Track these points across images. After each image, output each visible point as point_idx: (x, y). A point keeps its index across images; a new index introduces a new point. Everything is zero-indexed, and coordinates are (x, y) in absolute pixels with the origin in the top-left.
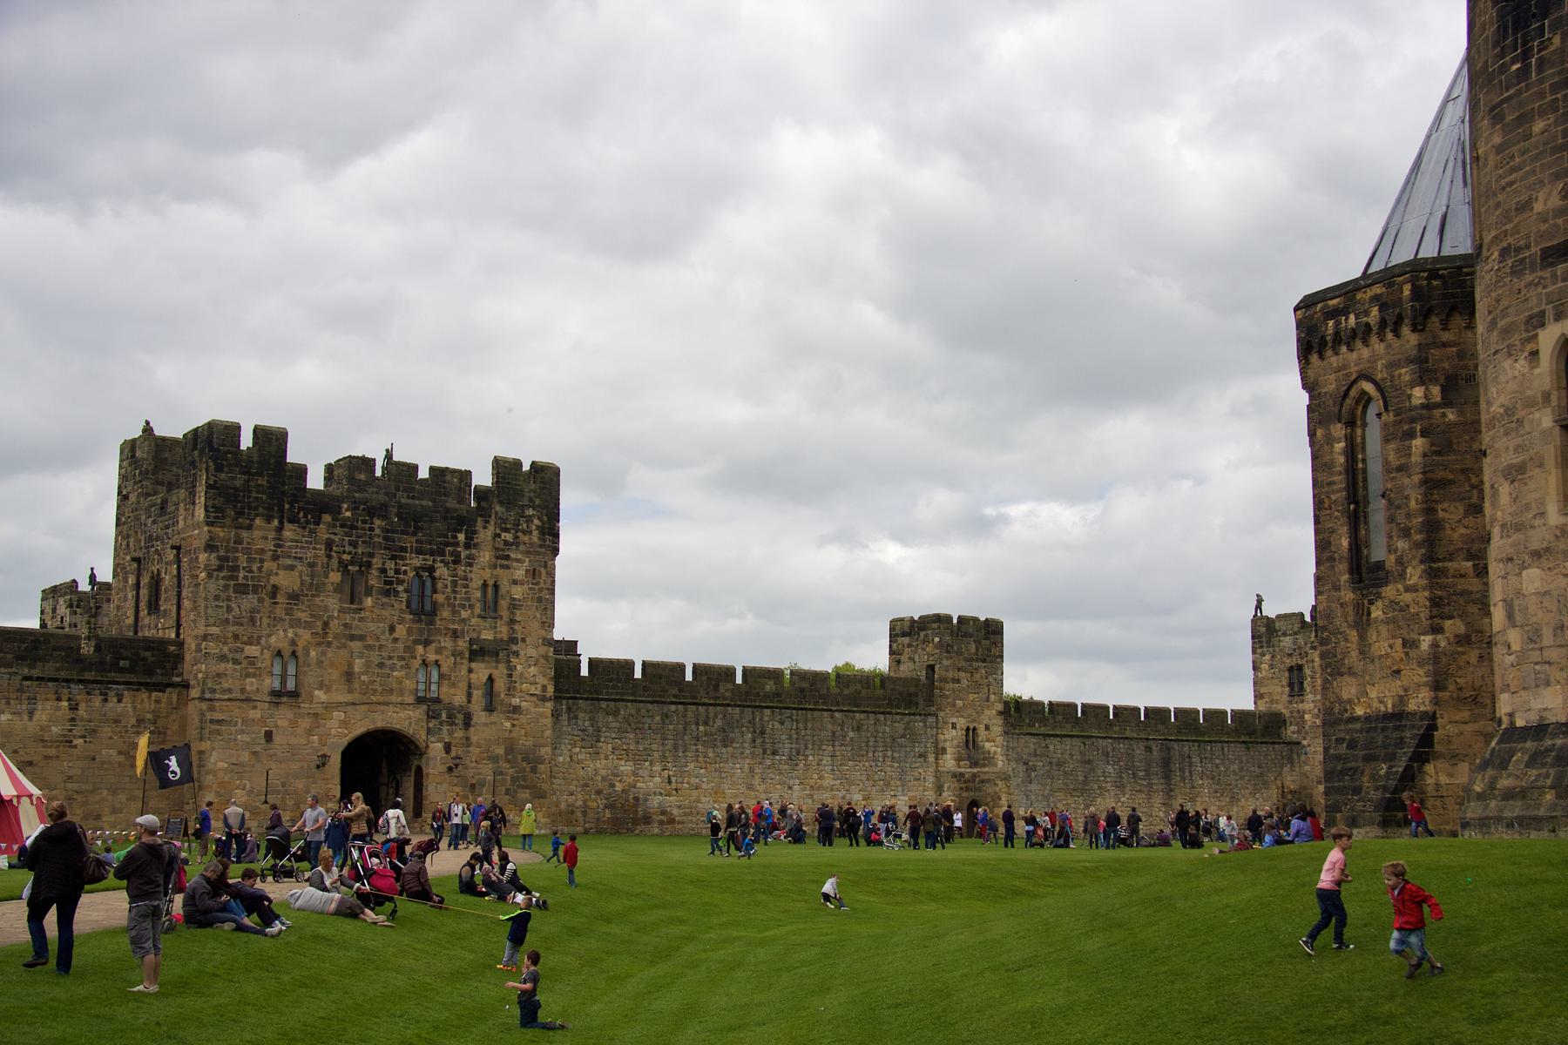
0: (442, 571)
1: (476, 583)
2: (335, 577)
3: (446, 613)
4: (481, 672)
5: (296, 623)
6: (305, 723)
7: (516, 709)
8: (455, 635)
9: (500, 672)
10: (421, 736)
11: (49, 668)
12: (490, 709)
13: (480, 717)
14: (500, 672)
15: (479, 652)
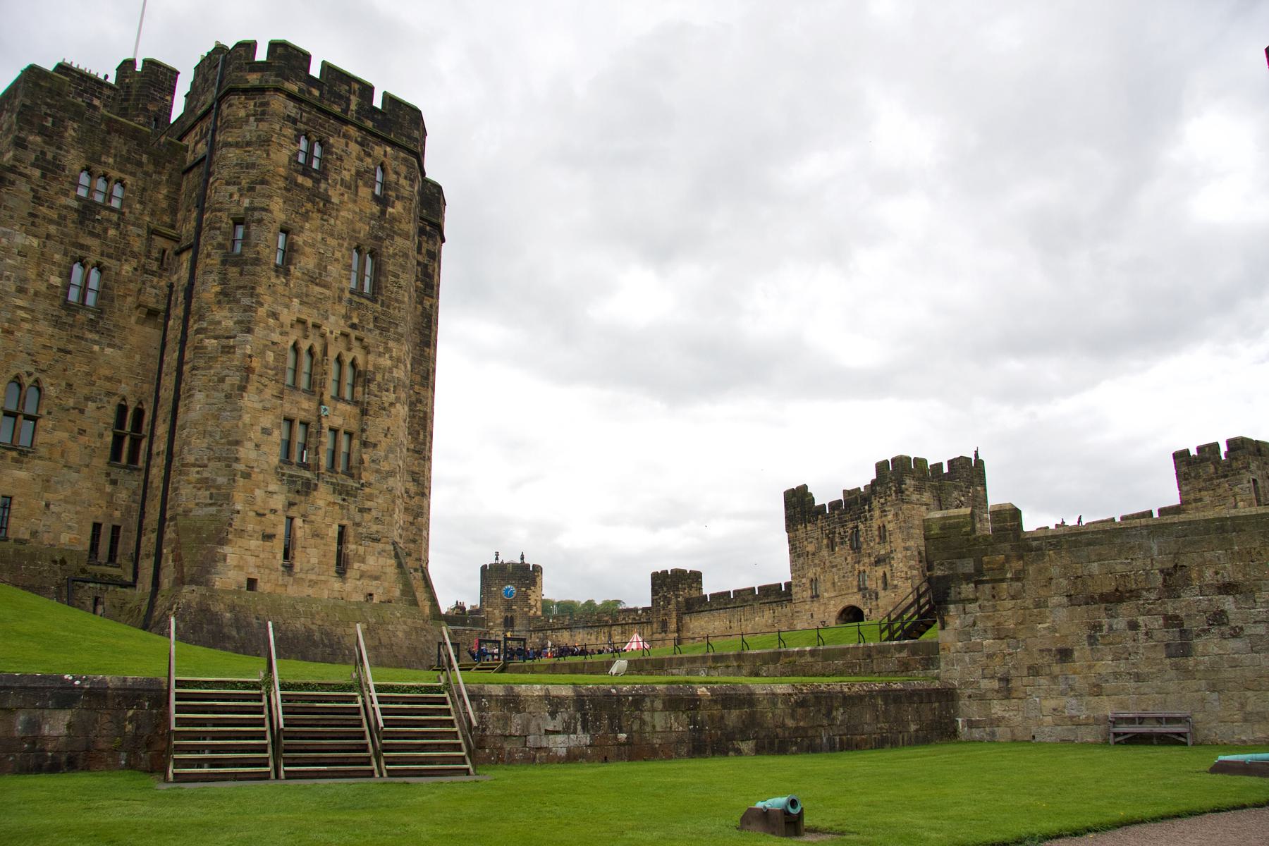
0: (861, 526)
1: (875, 527)
2: (825, 542)
3: (865, 546)
4: (880, 571)
5: (815, 565)
6: (822, 608)
7: (896, 586)
8: (869, 555)
9: (887, 569)
10: (861, 607)
11: (772, 599)
12: (885, 589)
13: (882, 593)
14: (887, 569)
15: (879, 561)
